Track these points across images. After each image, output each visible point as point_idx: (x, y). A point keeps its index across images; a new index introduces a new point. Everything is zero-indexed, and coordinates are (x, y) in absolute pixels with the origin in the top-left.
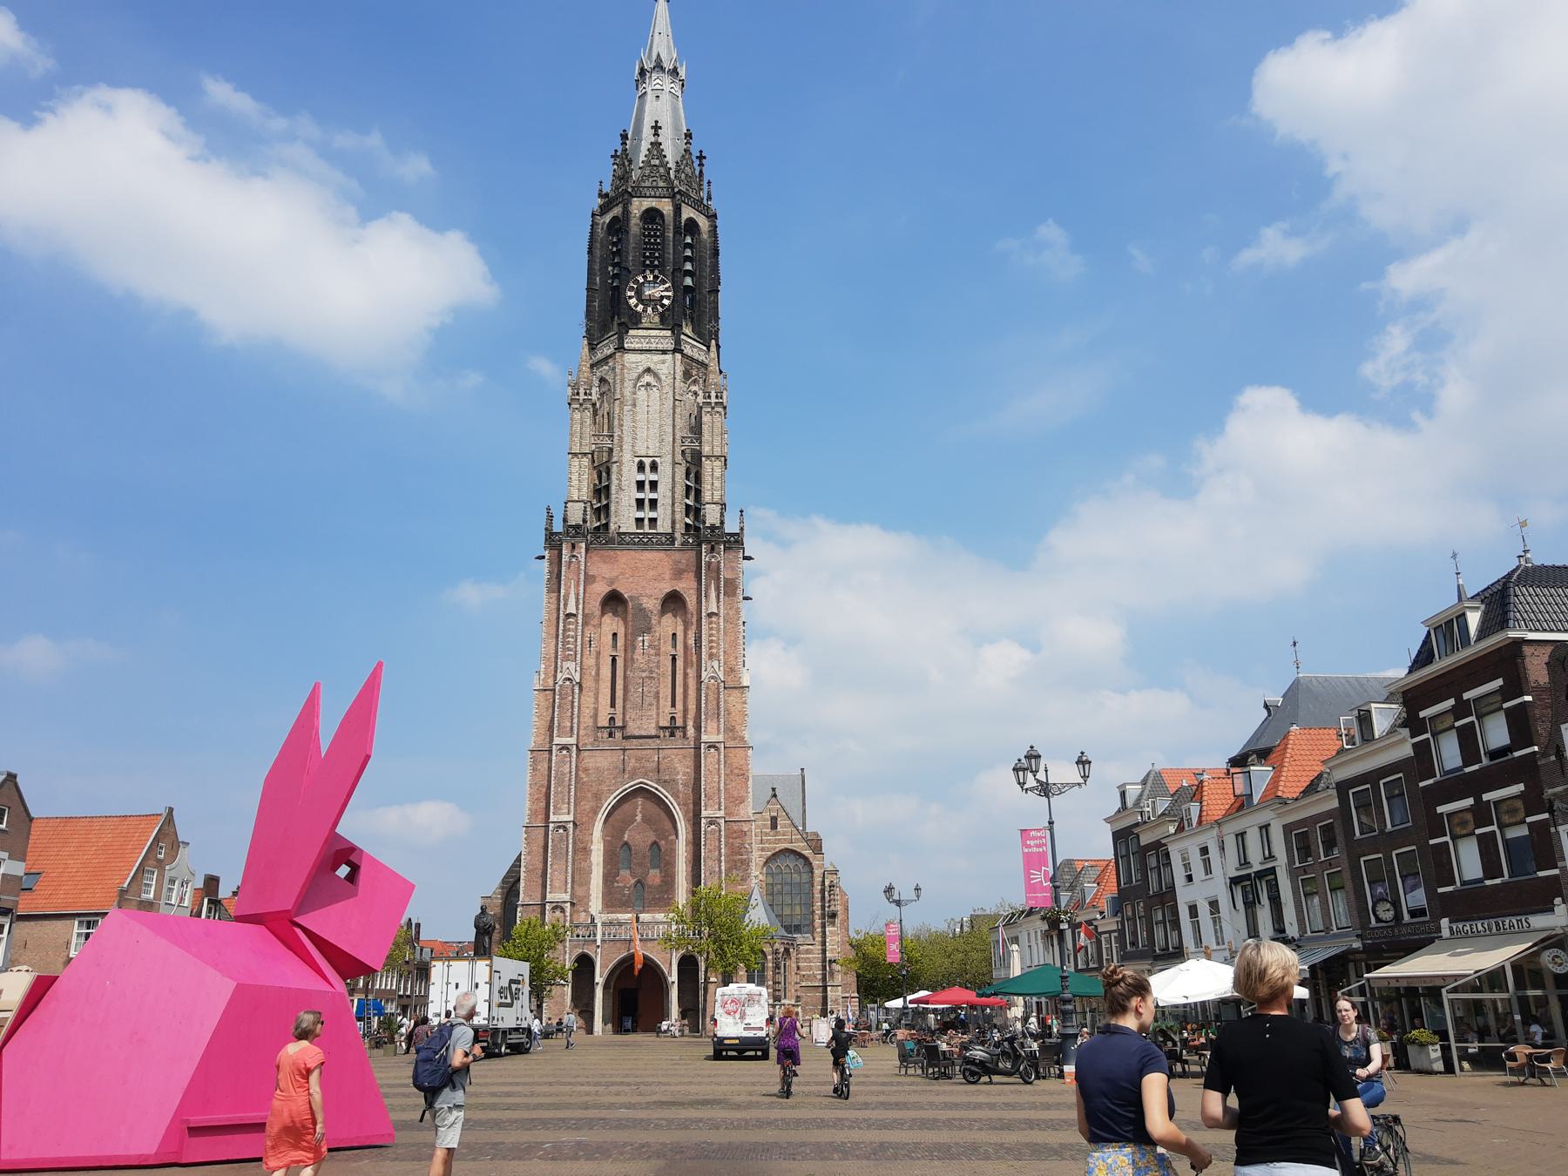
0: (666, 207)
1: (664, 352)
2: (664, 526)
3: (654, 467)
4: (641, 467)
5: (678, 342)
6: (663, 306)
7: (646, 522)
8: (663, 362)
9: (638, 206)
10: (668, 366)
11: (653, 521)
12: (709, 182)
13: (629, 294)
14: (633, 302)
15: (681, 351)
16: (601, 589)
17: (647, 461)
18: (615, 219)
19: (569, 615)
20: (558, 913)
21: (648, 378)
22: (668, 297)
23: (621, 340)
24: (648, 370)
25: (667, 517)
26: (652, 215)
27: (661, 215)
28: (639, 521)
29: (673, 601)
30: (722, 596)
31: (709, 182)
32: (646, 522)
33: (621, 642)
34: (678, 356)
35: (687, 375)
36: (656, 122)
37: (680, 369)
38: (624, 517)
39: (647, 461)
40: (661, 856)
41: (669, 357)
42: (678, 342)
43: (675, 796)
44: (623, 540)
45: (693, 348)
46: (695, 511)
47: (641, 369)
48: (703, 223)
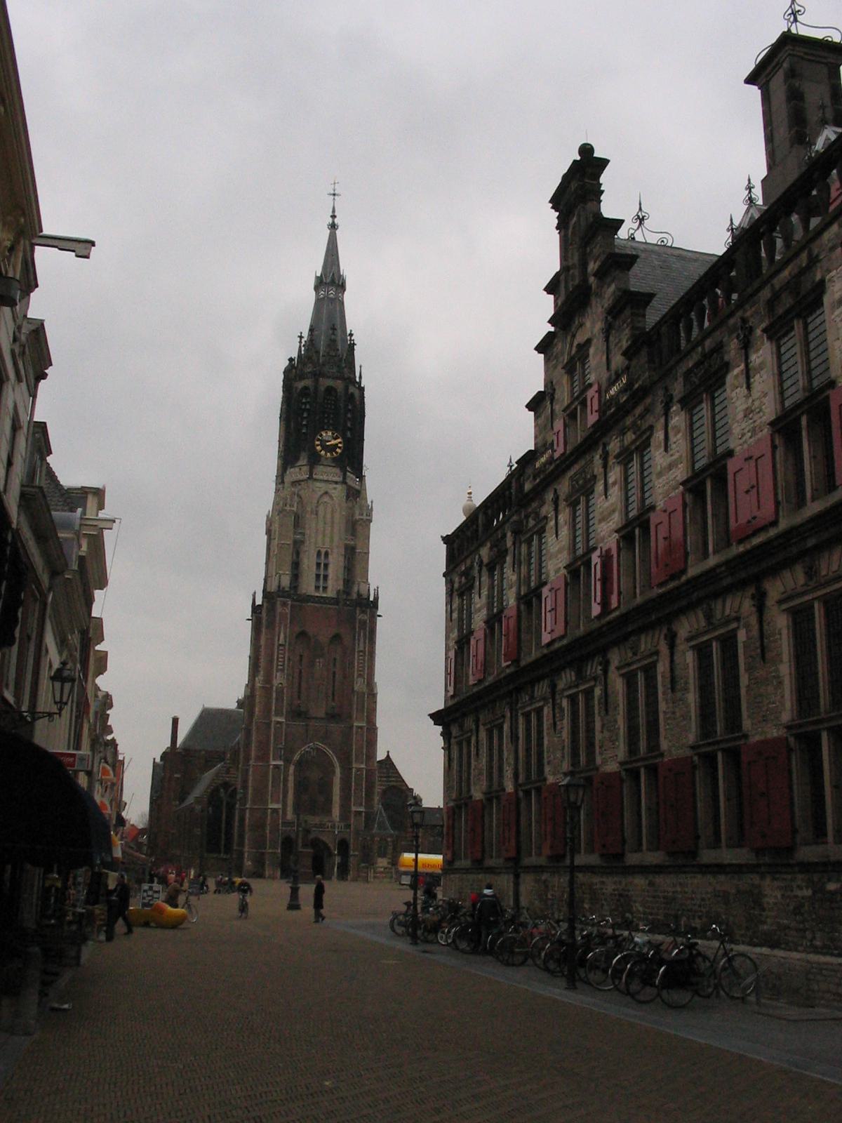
0: (339, 385)
1: (336, 483)
2: (330, 593)
3: (327, 554)
4: (319, 553)
5: (344, 478)
6: (337, 453)
7: (321, 589)
8: (335, 489)
9: (325, 383)
10: (338, 492)
11: (325, 588)
12: (361, 367)
13: (317, 443)
14: (319, 448)
15: (346, 483)
16: (297, 629)
17: (323, 551)
18: (306, 388)
19: (280, 645)
20: (275, 815)
21: (326, 499)
22: (340, 448)
23: (311, 474)
24: (326, 493)
25: (333, 586)
26: (330, 390)
27: (335, 390)
28: (317, 588)
29: (337, 638)
30: (367, 641)
31: (361, 367)
32: (321, 589)
33: (305, 660)
34: (344, 486)
35: (348, 497)
36: (334, 325)
37: (344, 494)
38: (308, 586)
39: (323, 551)
40: (325, 788)
41: (339, 487)
42: (344, 478)
43: (336, 754)
44: (309, 598)
45: (352, 480)
46: (348, 582)
47: (320, 493)
48: (357, 393)
